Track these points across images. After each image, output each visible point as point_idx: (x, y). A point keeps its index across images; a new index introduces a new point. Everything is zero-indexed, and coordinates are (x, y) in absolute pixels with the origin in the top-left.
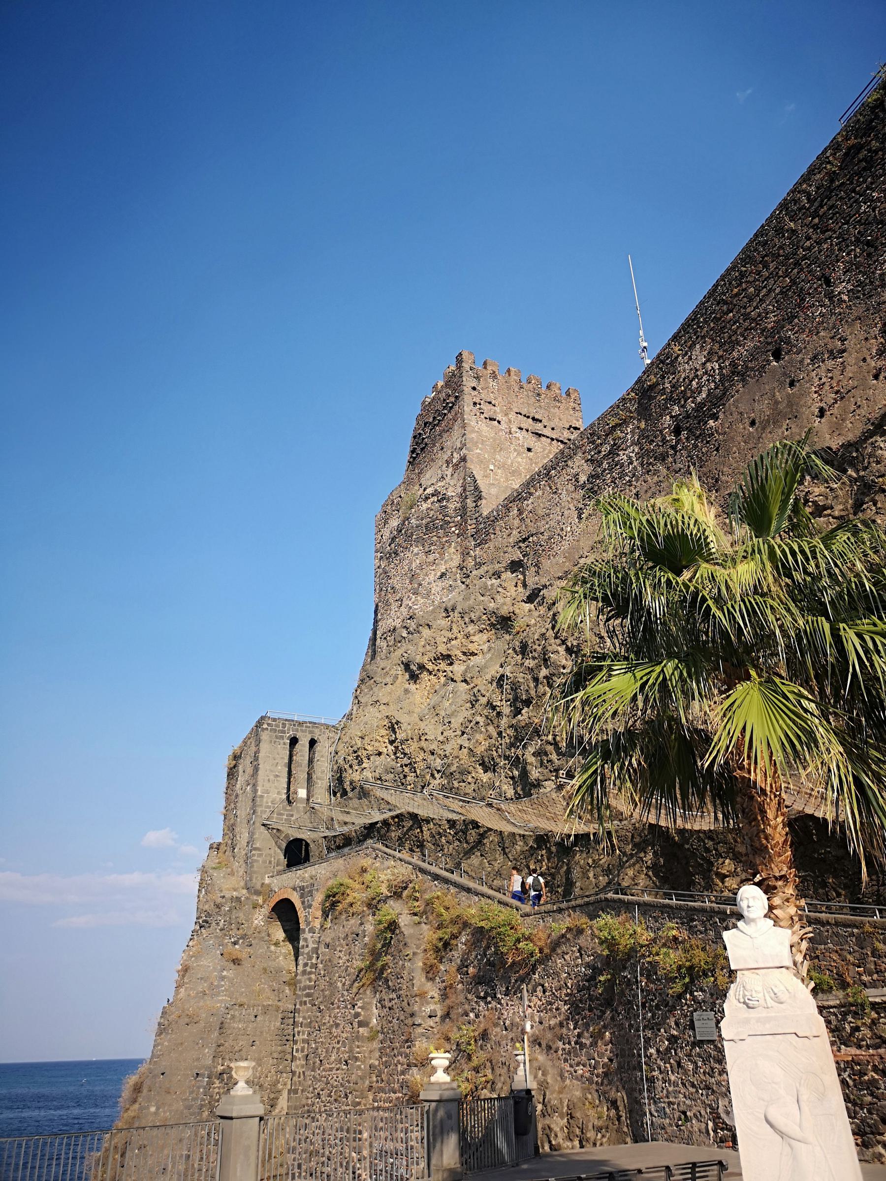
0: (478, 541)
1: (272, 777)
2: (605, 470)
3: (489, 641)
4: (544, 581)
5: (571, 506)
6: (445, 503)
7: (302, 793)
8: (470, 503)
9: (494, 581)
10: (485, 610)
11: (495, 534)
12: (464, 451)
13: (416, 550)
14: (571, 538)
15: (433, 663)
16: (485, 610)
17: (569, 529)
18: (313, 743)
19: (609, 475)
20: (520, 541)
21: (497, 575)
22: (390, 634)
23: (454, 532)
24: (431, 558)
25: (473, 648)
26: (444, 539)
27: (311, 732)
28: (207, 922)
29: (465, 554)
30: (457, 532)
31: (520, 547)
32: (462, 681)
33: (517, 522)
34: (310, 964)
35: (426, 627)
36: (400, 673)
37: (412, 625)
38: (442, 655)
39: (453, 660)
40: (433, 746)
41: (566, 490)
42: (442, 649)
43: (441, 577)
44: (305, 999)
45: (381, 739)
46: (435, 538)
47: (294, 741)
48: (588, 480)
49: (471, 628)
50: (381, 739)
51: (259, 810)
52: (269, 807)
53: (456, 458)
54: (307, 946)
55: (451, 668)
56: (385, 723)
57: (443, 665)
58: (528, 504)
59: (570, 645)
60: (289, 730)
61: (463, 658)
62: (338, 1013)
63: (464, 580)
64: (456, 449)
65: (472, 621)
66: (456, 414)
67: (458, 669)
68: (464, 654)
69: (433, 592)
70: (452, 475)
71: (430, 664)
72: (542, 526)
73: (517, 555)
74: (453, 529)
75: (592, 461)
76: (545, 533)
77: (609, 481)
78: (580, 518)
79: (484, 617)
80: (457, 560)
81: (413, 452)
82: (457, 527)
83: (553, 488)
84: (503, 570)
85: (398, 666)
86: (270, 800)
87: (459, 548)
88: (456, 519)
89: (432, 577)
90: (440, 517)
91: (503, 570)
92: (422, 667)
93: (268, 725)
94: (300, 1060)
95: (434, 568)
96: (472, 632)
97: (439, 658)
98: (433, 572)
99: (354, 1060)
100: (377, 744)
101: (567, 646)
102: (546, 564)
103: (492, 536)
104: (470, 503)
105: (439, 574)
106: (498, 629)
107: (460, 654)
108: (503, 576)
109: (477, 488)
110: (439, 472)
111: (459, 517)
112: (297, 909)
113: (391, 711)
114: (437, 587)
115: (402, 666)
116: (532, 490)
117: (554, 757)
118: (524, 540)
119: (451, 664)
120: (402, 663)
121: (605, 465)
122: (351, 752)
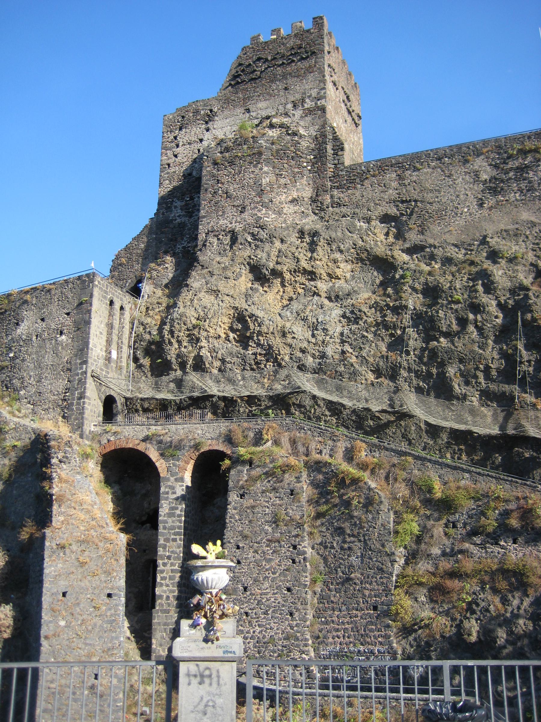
0: (336, 184)
1: (98, 333)
2: (510, 179)
3: (352, 271)
4: (431, 241)
5: (469, 193)
6: (296, 139)
7: (114, 355)
8: (329, 148)
9: (362, 224)
10: (355, 245)
11: (362, 185)
12: (323, 102)
13: (265, 169)
14: (468, 217)
15: (291, 274)
16: (355, 245)
17: (466, 210)
18: (122, 308)
19: (515, 185)
20: (398, 201)
21: (368, 220)
22: (223, 233)
23: (305, 167)
24: (282, 181)
25: (339, 272)
26: (296, 170)
27: (121, 300)
28: (67, 458)
29: (319, 191)
30: (309, 168)
31: (398, 206)
32: (326, 297)
33: (394, 184)
34: (180, 509)
35: (279, 240)
36: (244, 271)
37: (263, 235)
38: (304, 269)
39: (316, 277)
40: (305, 345)
41: (463, 179)
42: (304, 264)
43: (292, 201)
44: (172, 537)
45: (222, 325)
46: (286, 165)
47: (112, 303)
48: (490, 180)
49: (338, 255)
50: (222, 325)
51: (90, 361)
52: (95, 360)
53: (309, 104)
54: (174, 493)
55: (312, 283)
56: (231, 313)
57: (301, 279)
58: (411, 176)
59: (503, 302)
60: (110, 292)
61: (327, 278)
62: (268, 550)
63: (317, 212)
64: (309, 97)
65: (341, 251)
66: (310, 67)
67: (323, 286)
68: (329, 275)
69: (285, 212)
70: (302, 117)
71: (288, 274)
72: (429, 197)
73: (393, 211)
74: (305, 164)
75: (496, 166)
76: (434, 204)
77: (516, 188)
78: (481, 205)
79: (352, 250)
80: (308, 193)
81: (235, 77)
82: (310, 164)
83: (446, 172)
84: (374, 218)
85: (243, 266)
86: (96, 355)
87: (311, 182)
88: (308, 157)
89: (283, 197)
90: (292, 149)
91: (374, 218)
92: (276, 273)
93: (99, 282)
94: (167, 586)
95: (286, 190)
96: (339, 259)
97: (299, 272)
98: (284, 195)
99: (303, 586)
100: (218, 329)
101: (499, 301)
102: (436, 229)
103: (359, 186)
104: (329, 148)
105: (290, 198)
106: (366, 265)
107: (325, 274)
108: (373, 223)
109: (336, 139)
110: (280, 107)
111: (312, 157)
112: (154, 460)
113: (242, 304)
114: (289, 209)
115: (248, 267)
116: (418, 165)
117: (482, 380)
118: (403, 202)
119: (312, 280)
120: (249, 264)
121: (511, 174)
122: (183, 329)
